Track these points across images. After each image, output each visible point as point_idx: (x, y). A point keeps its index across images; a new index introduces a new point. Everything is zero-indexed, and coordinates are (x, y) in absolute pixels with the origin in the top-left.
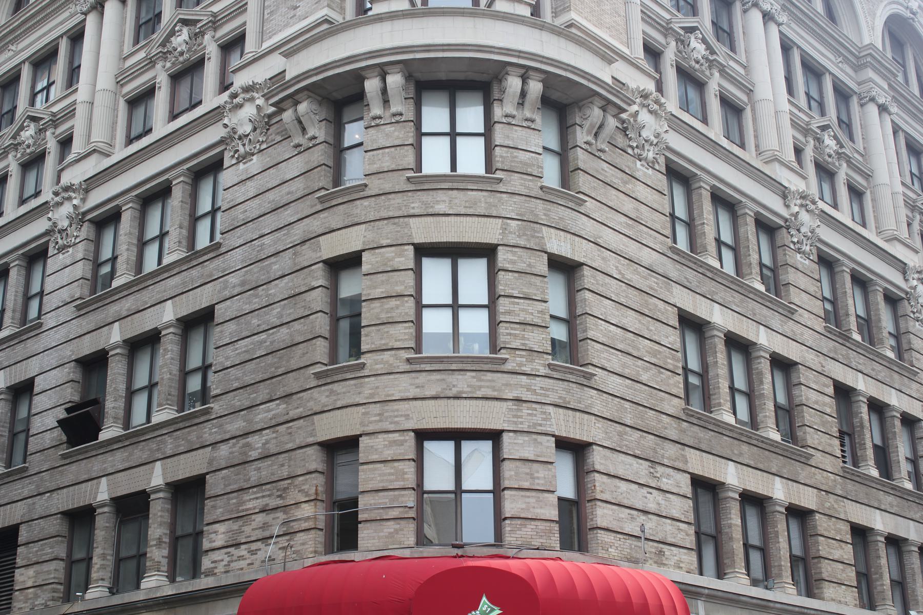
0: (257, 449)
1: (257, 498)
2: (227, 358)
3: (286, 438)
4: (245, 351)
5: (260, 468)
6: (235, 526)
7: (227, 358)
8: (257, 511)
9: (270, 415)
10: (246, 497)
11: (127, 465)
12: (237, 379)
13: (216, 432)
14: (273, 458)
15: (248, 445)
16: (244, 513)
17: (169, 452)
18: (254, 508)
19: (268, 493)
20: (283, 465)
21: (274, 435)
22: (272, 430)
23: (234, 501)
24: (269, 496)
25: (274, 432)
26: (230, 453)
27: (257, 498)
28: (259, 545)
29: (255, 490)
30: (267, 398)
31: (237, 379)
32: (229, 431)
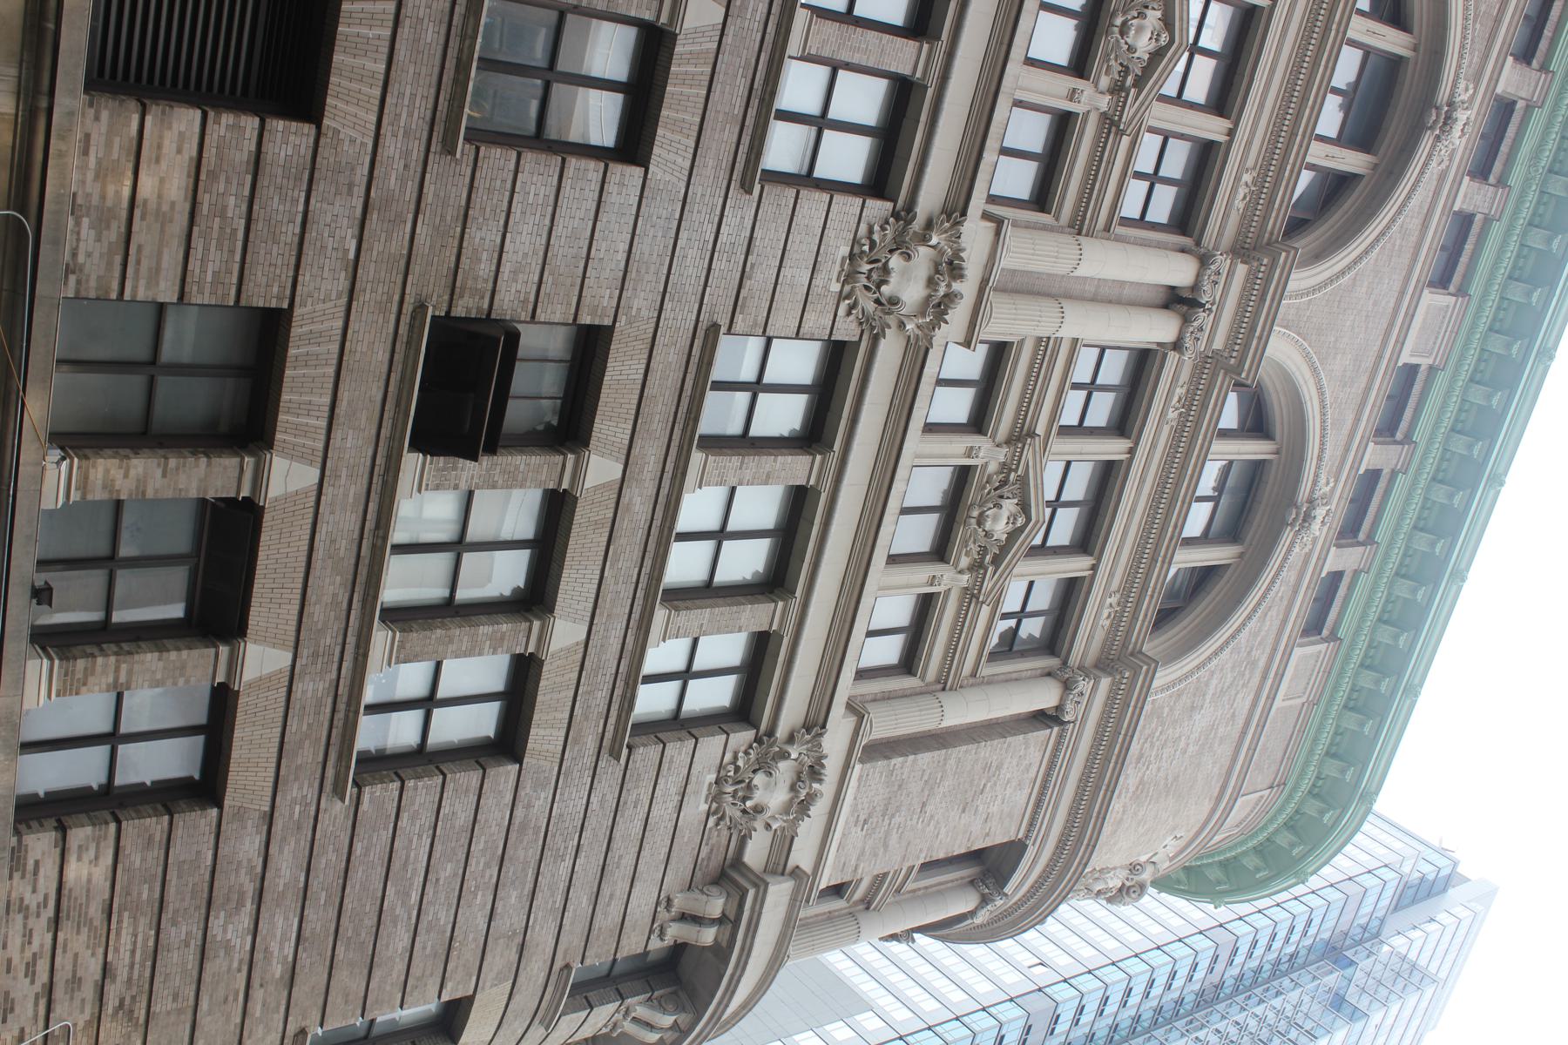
0: (225, 931)
1: (133, 952)
2: (413, 818)
3: (221, 993)
4: (408, 857)
5: (187, 945)
6: (95, 911)
7: (413, 818)
8: (110, 958)
9: (274, 947)
10: (144, 922)
11: (319, 554)
12: (367, 850)
13: (292, 815)
14: (195, 974)
15: (240, 904)
16: (114, 926)
17: (298, 687)
18: (117, 950)
19: (136, 976)
20: (175, 997)
21: (235, 965)
22: (247, 957)
23: (145, 896)
24: (130, 979)
25: (241, 961)
26: (240, 863)
27: (133, 952)
28: (43, 976)
29: (151, 943)
30: (307, 932)
31: (367, 850)
32: (281, 851)
